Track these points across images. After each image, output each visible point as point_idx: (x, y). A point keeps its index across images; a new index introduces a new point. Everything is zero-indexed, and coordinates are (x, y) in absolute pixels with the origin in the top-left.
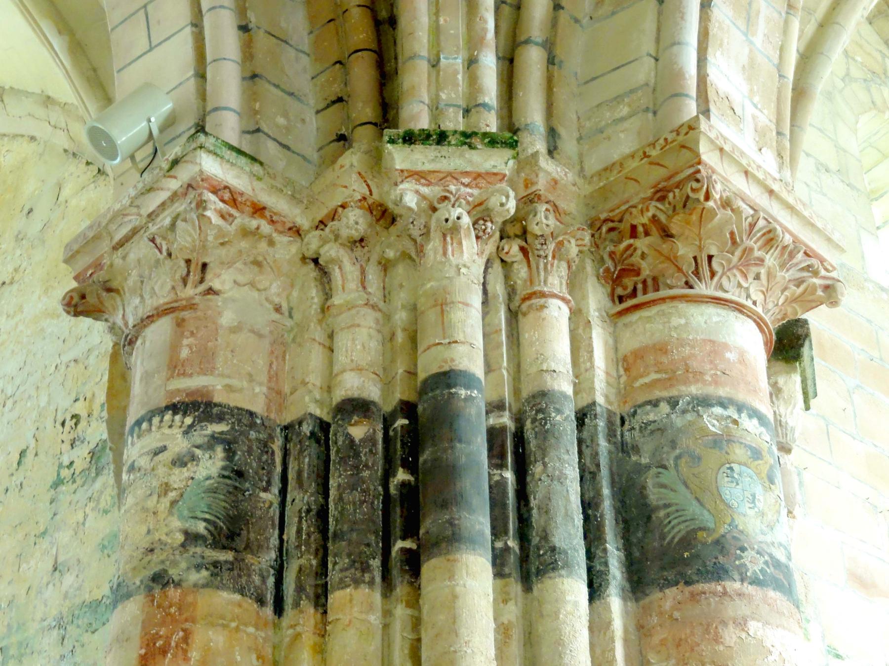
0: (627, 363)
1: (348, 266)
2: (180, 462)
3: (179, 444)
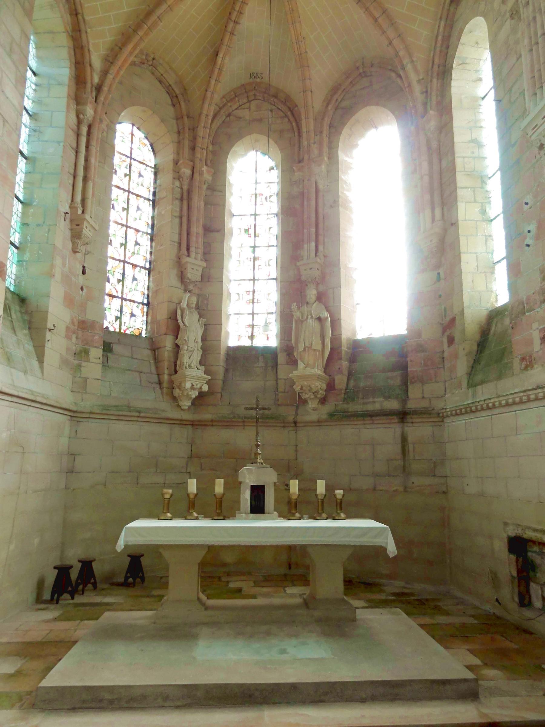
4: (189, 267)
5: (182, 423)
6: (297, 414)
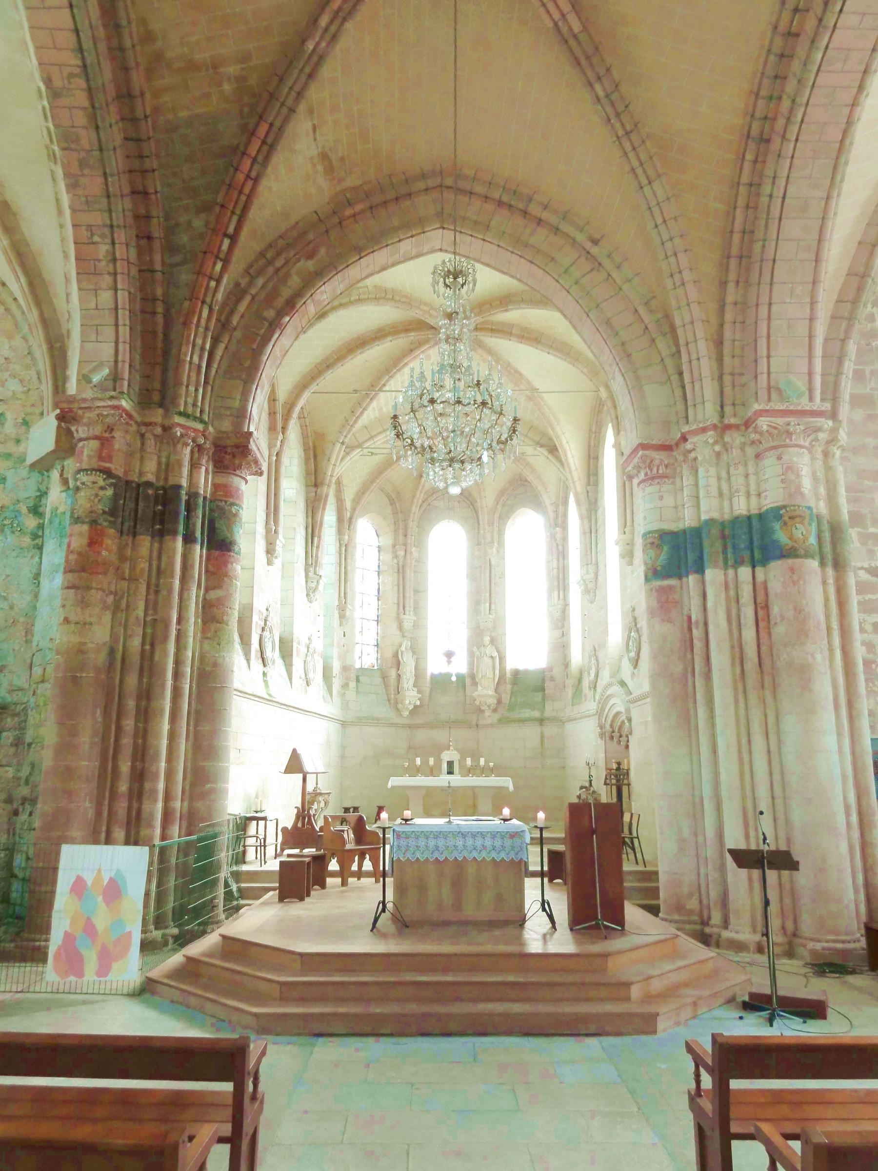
0: (216, 486)
1: (153, 441)
2: (102, 488)
3: (101, 483)
4: (405, 621)
5: (403, 726)
6: (478, 720)
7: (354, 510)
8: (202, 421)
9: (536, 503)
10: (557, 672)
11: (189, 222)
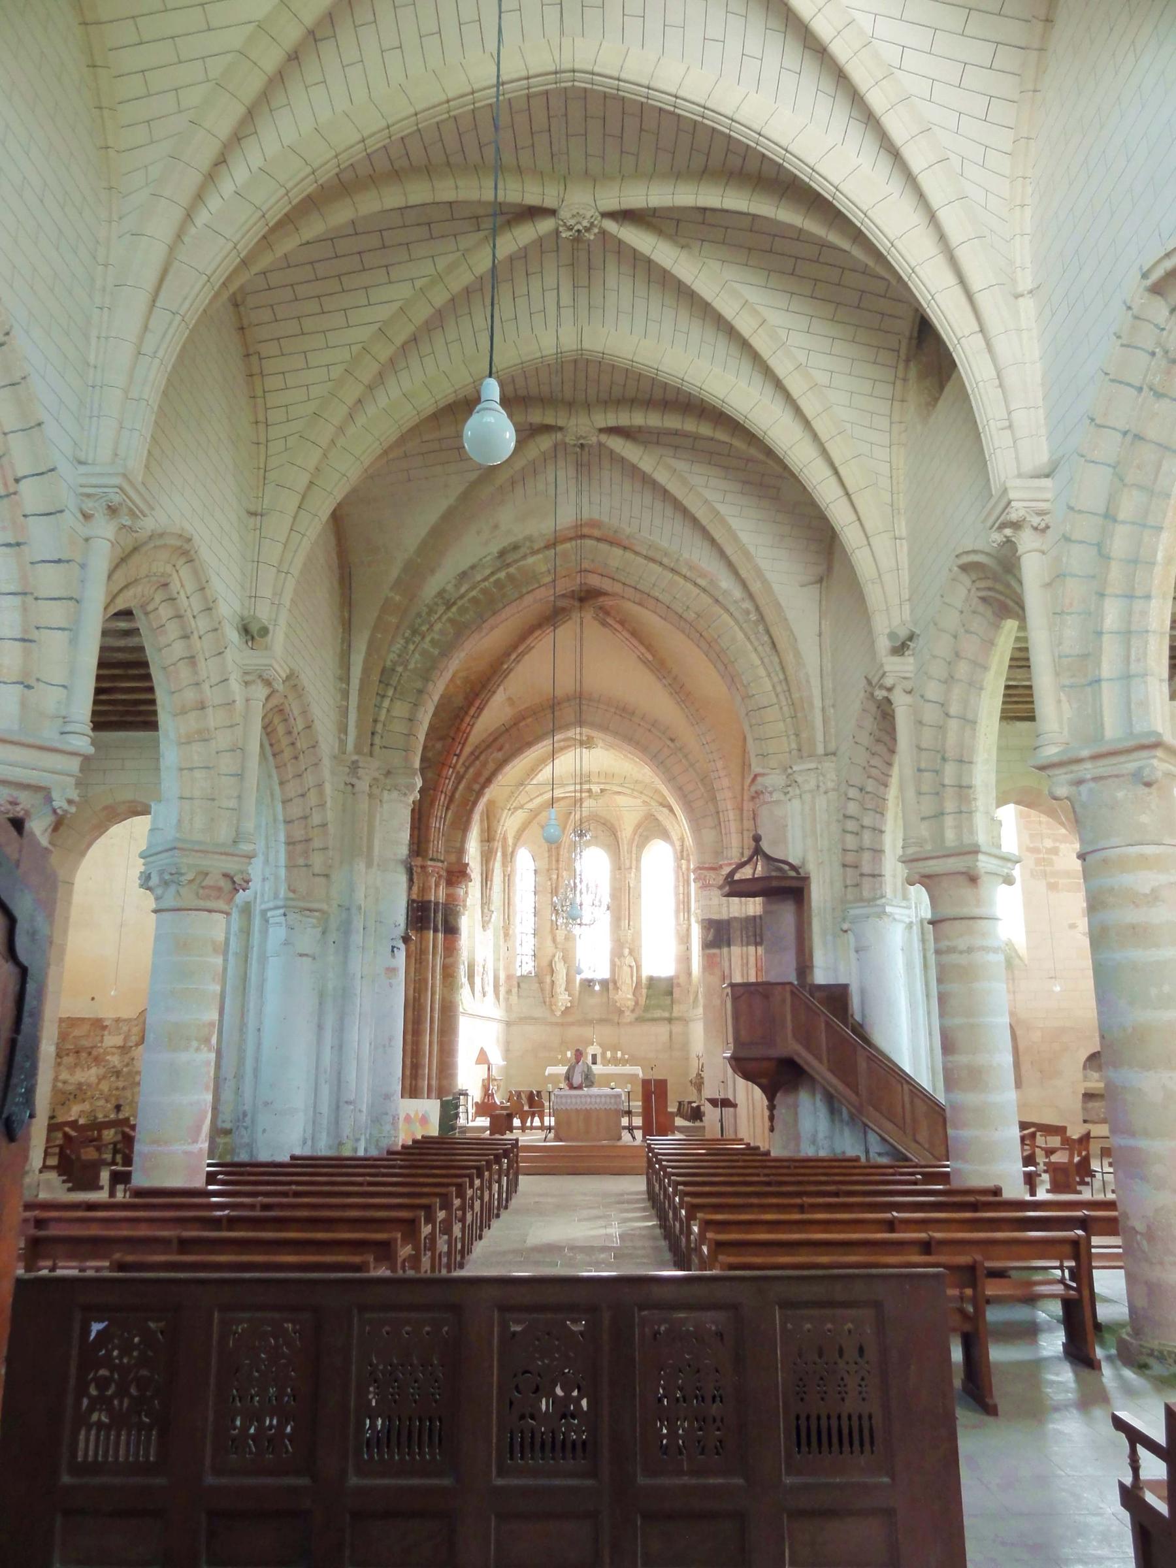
7: (515, 845)
8: (443, 862)
9: (665, 835)
10: (682, 980)
11: (433, 746)
